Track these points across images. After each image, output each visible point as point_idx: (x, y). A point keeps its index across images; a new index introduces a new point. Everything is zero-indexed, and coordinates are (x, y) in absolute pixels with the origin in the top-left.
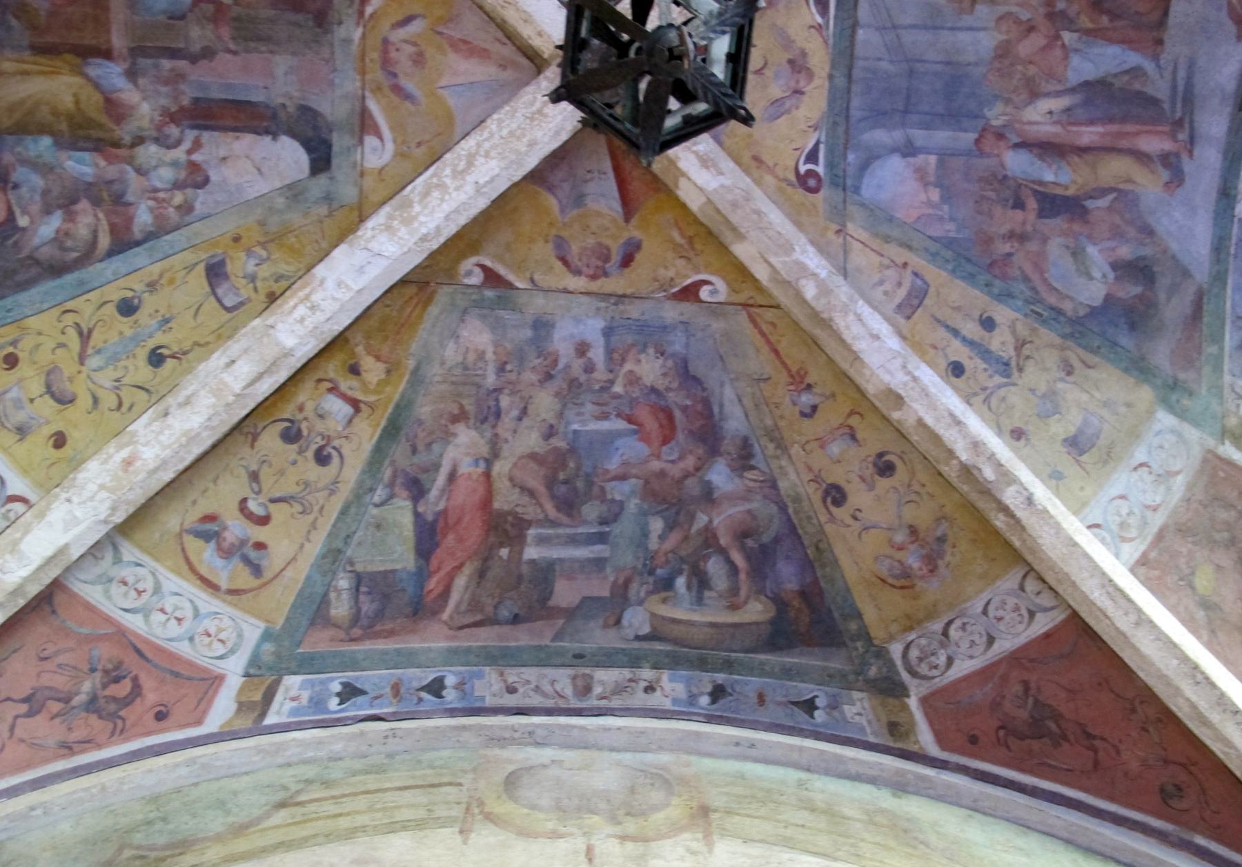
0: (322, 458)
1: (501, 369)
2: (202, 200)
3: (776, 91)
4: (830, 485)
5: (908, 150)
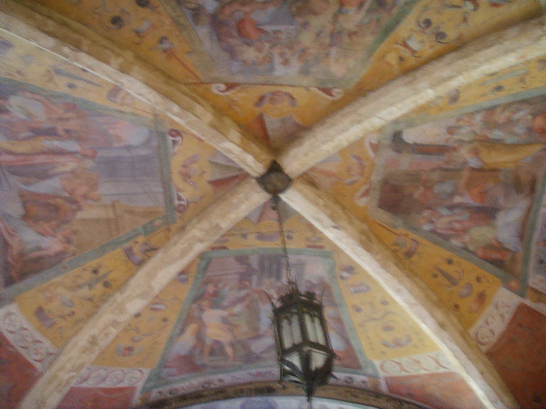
0: (428, 23)
1: (327, 55)
2: (452, 122)
3: (195, 166)
4: (146, 6)
5: (128, 148)
